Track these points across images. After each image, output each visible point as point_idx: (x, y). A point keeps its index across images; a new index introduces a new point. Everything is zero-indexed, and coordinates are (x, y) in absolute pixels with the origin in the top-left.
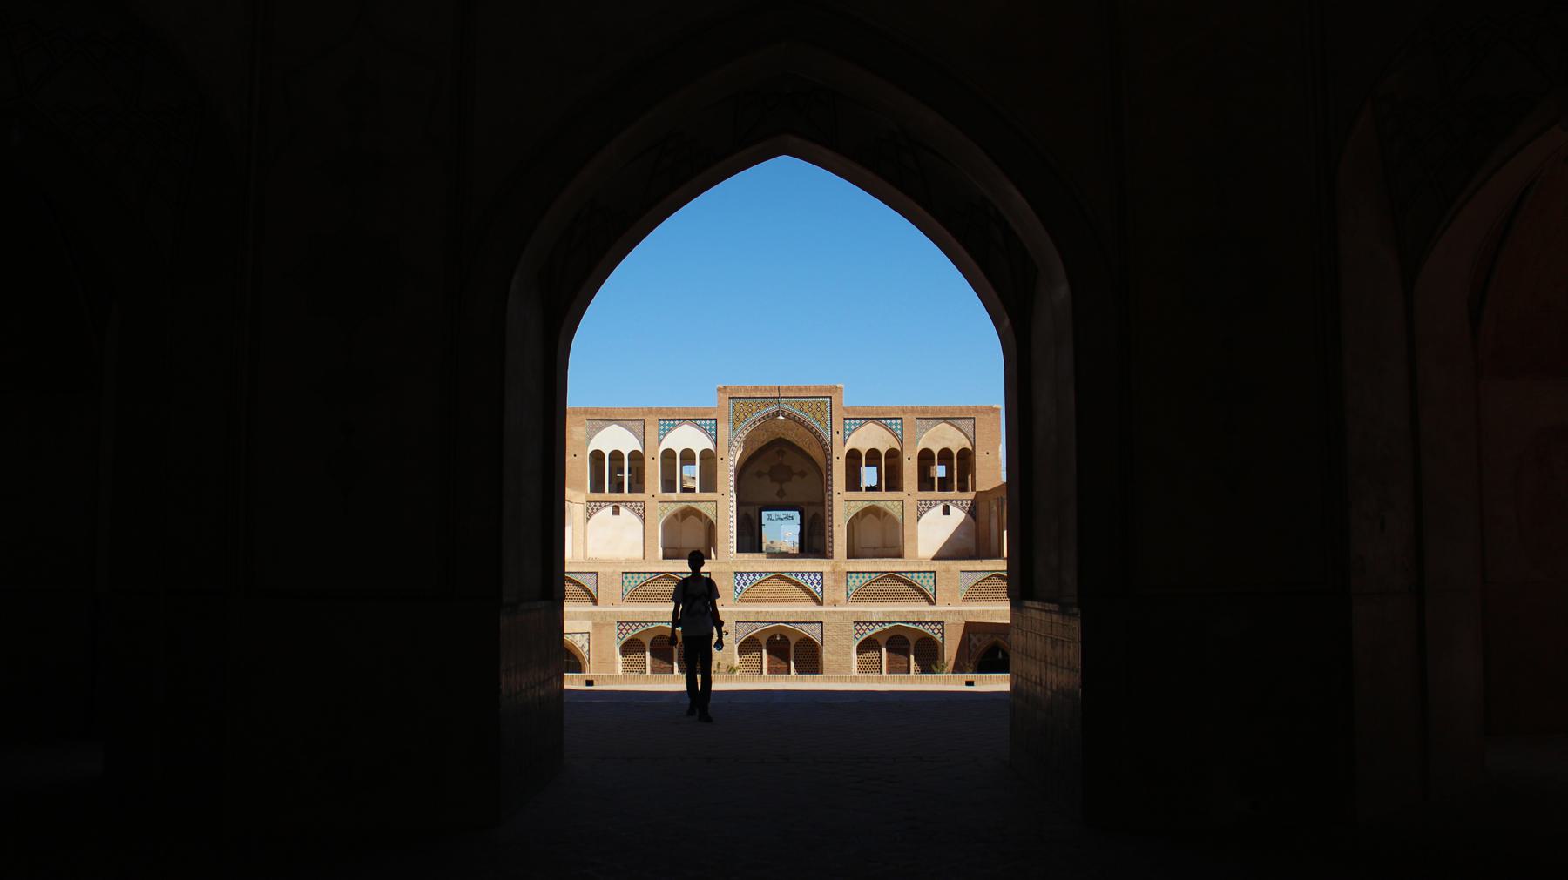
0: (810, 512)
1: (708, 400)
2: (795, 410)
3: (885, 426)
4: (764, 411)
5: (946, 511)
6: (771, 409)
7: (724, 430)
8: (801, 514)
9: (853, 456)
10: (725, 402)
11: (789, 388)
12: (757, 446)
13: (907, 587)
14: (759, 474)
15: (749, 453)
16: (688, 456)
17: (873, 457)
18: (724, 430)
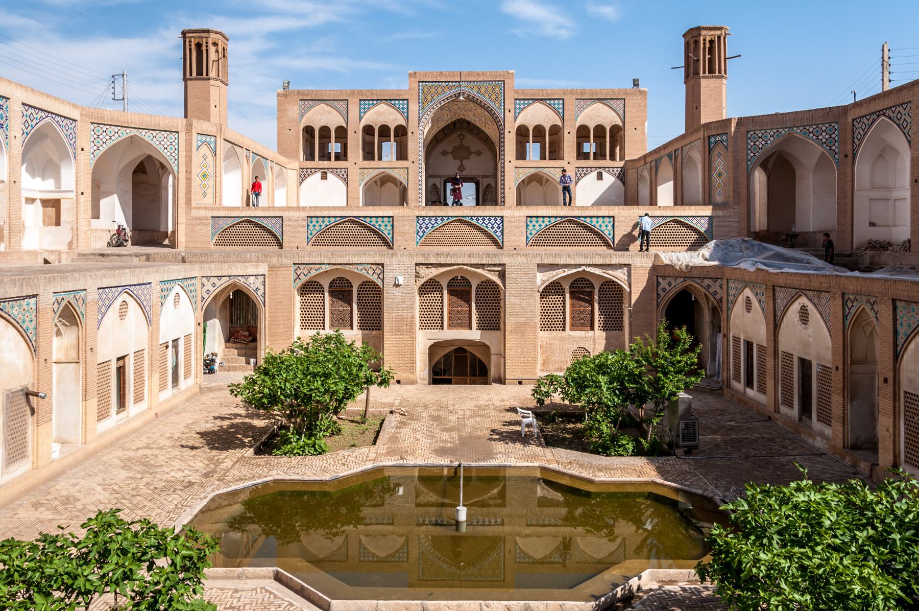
0: (484, 183)
1: (400, 84)
2: (474, 93)
3: (549, 106)
4: (448, 93)
5: (600, 177)
6: (454, 91)
7: (414, 108)
8: (477, 184)
9: (522, 132)
10: (415, 85)
11: (469, 74)
12: (442, 125)
13: (583, 229)
14: (444, 153)
15: (436, 130)
16: (384, 131)
17: (539, 131)
18: (414, 108)
